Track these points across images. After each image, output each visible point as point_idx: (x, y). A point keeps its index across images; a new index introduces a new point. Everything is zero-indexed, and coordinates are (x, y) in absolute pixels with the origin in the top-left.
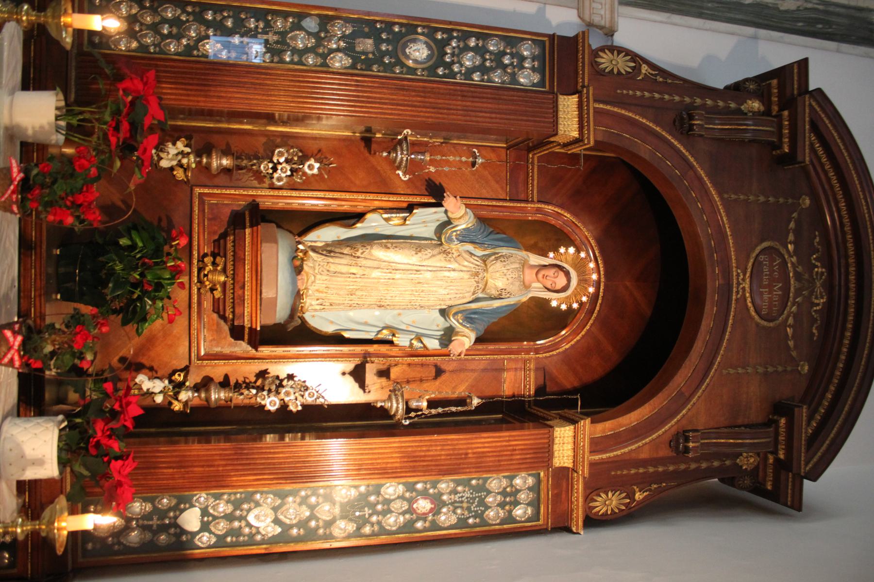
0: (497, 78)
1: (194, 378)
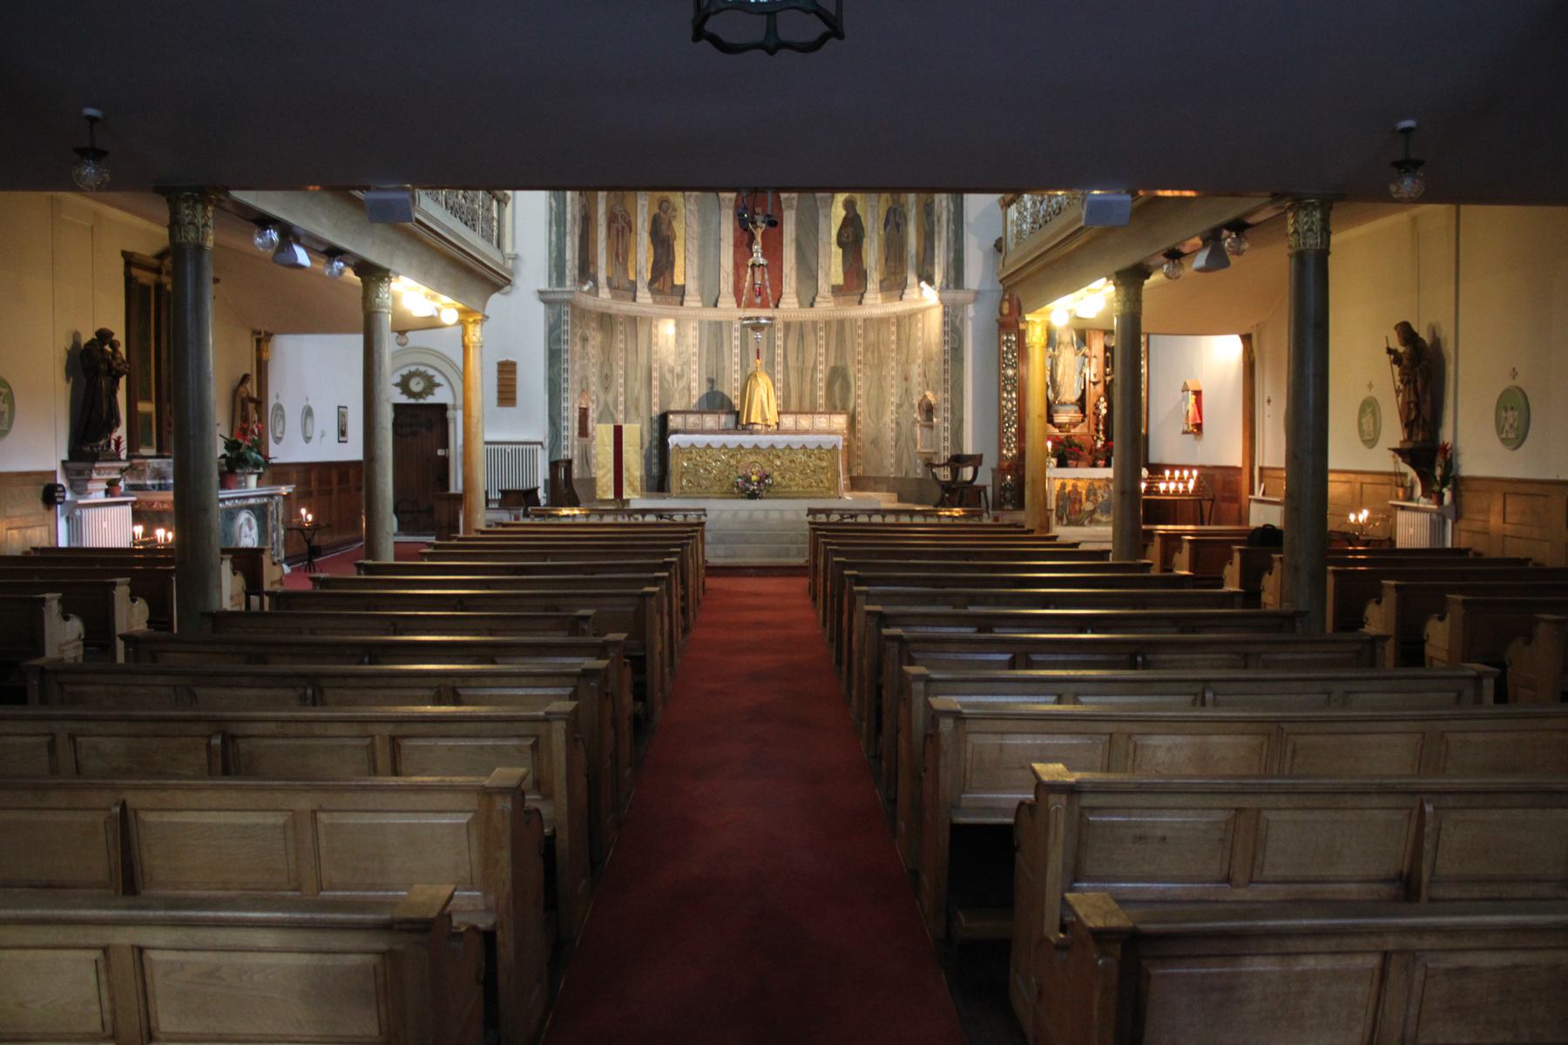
0: (1014, 347)
1: (1095, 433)
